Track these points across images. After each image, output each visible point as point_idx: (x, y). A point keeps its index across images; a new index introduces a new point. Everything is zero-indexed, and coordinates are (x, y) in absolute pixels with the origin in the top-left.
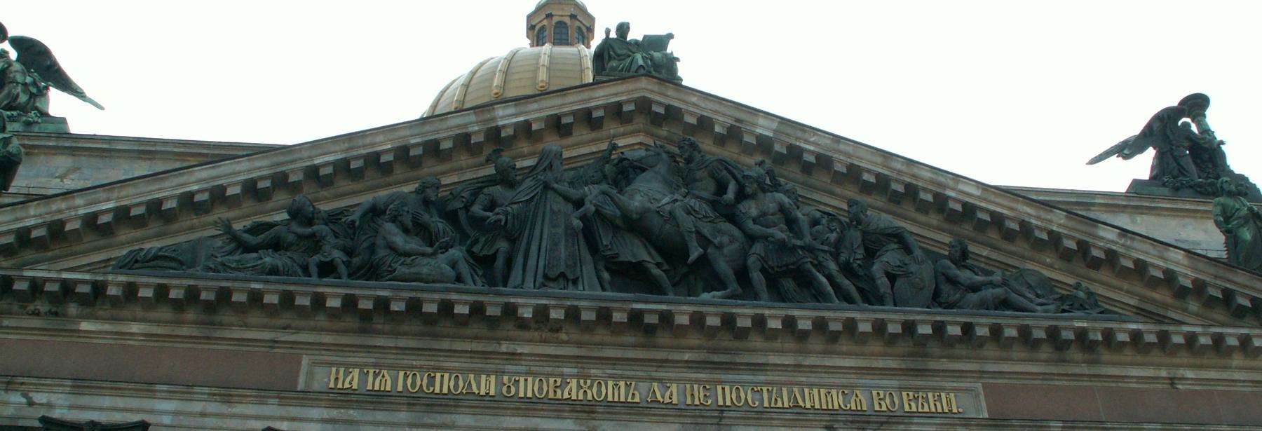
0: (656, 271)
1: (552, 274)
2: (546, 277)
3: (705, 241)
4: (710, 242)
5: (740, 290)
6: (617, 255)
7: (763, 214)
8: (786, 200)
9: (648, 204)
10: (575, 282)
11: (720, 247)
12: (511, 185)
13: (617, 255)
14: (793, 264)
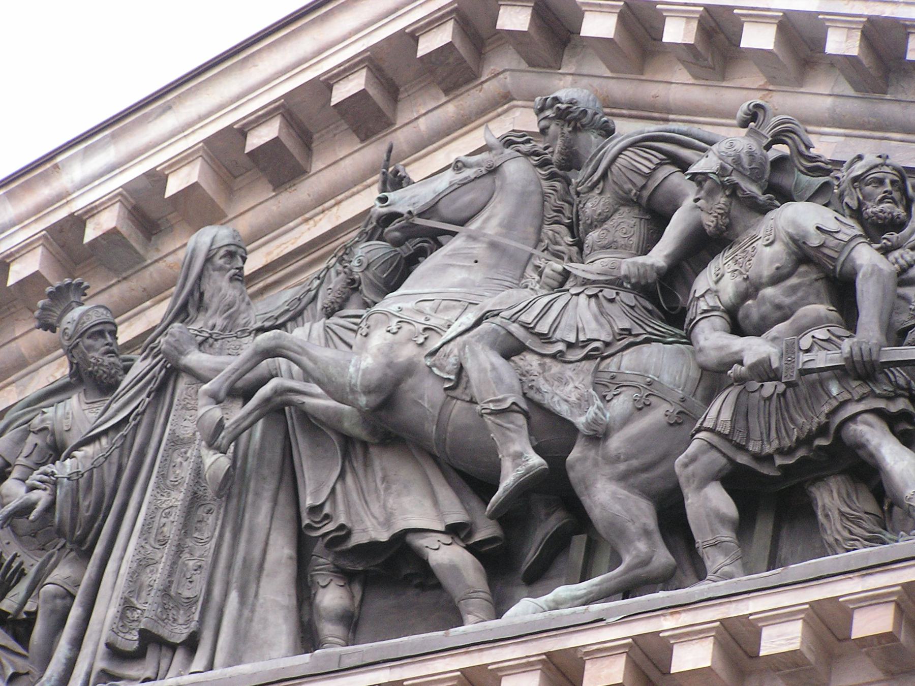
0: (445, 555)
1: (130, 641)
2: (115, 653)
3: (554, 433)
4: (571, 429)
5: (663, 557)
6: (344, 532)
7: (751, 290)
8: (805, 217)
9: (407, 352)
10: (191, 645)
11: (598, 436)
12: (104, 386)
13: (344, 532)
14: (823, 430)
